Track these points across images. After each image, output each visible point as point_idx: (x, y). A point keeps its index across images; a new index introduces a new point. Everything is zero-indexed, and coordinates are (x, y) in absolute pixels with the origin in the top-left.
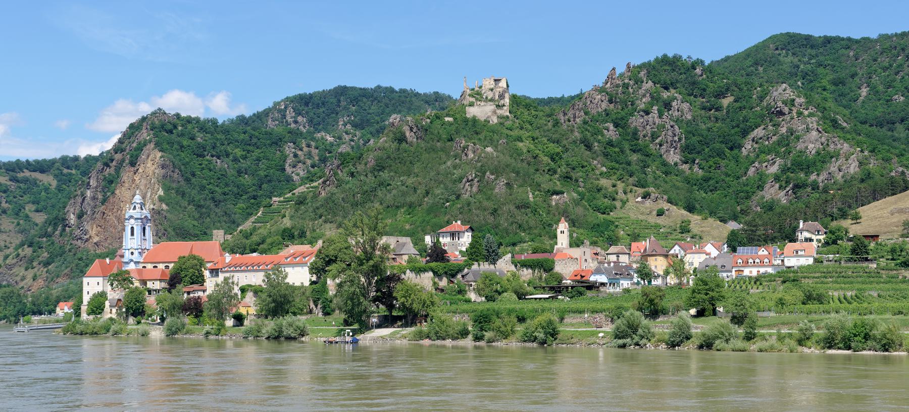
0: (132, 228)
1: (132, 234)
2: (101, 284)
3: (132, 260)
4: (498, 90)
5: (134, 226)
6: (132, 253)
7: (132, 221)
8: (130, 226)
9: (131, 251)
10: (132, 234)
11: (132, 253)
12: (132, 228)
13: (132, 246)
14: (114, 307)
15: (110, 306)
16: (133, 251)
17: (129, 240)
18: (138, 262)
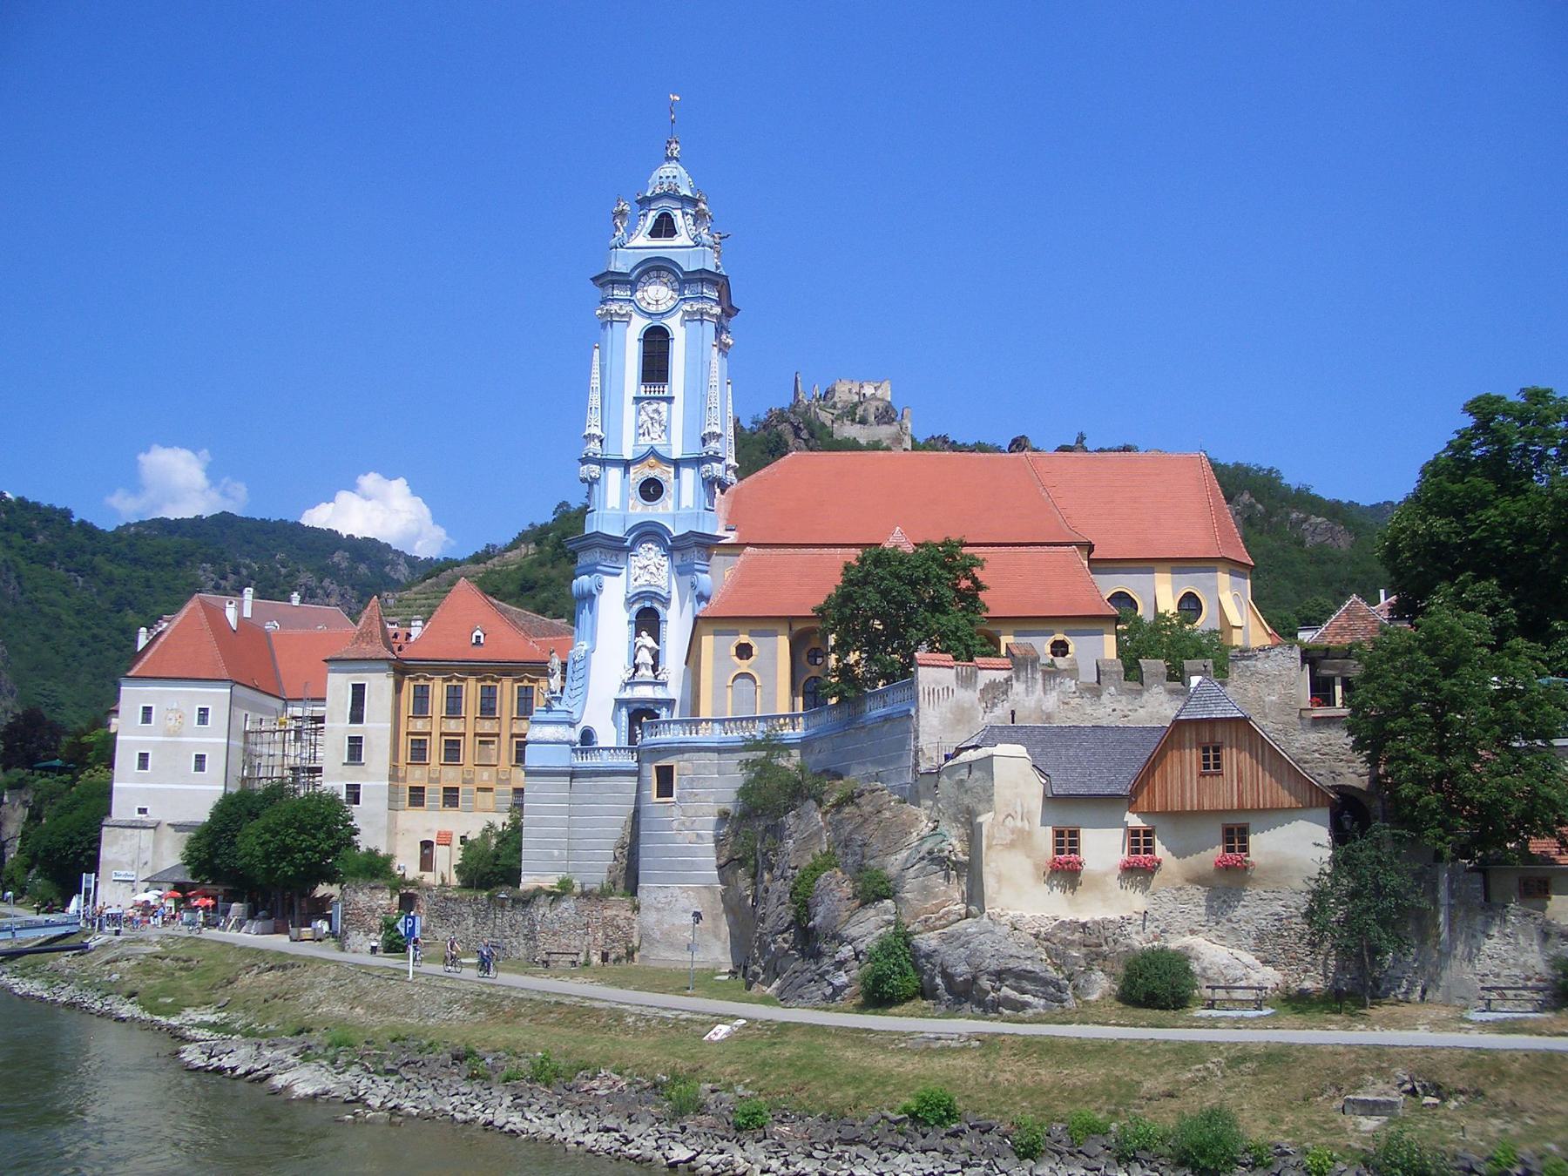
0: (656, 344)
1: (655, 365)
2: (218, 717)
3: (650, 533)
4: (875, 403)
5: (674, 324)
6: (651, 490)
7: (658, 294)
9: (638, 474)
10: (655, 365)
11: (651, 490)
12: (656, 344)
13: (656, 440)
14: (1104, 804)
15: (1053, 800)
16: (664, 474)
17: (630, 409)
18: (705, 544)
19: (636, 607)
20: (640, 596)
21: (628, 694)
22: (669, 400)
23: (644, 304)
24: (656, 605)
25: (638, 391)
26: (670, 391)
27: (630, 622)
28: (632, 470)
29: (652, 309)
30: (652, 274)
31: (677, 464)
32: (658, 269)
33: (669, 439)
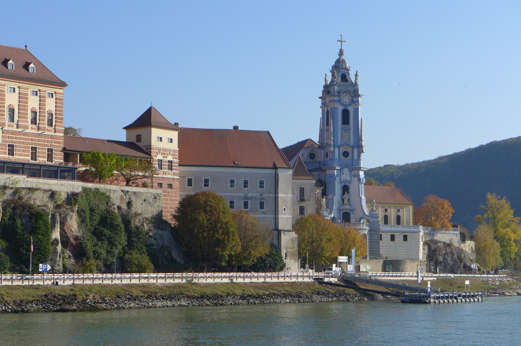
5: (351, 109)
8: (341, 108)
9: (342, 150)
19: (343, 184)
20: (344, 182)
21: (342, 208)
22: (349, 130)
23: (342, 102)
24: (348, 184)
25: (341, 126)
26: (350, 126)
27: (341, 188)
28: (341, 148)
29: (345, 104)
30: (345, 94)
31: (352, 147)
32: (346, 92)
33: (350, 141)
